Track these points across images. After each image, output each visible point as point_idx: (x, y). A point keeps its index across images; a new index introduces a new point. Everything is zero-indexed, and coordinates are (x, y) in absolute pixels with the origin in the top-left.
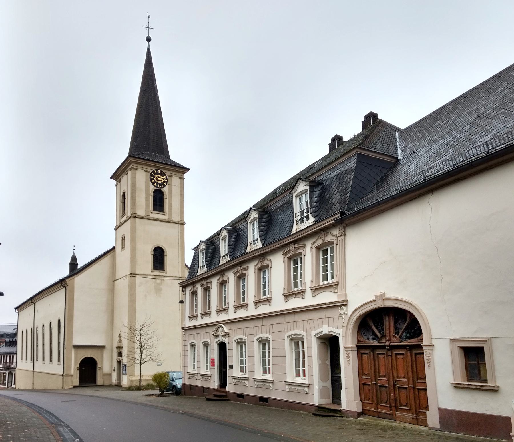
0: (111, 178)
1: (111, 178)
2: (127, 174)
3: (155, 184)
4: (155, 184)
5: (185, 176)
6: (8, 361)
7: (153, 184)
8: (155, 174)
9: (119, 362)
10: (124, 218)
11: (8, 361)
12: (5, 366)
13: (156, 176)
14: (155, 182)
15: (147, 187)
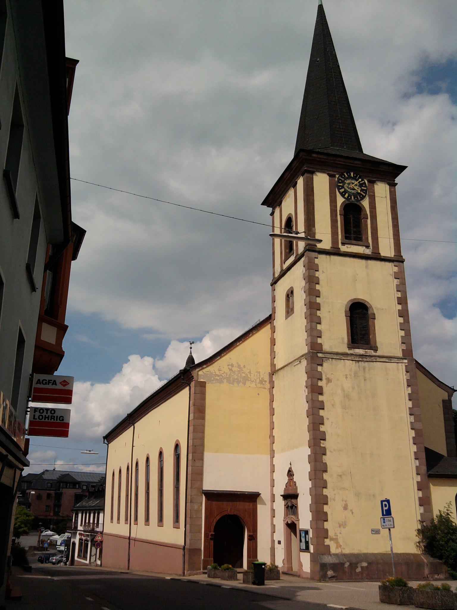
0: (263, 204)
1: (263, 204)
2: (295, 186)
3: (346, 195)
4: (346, 195)
5: (397, 180)
6: (91, 521)
7: (343, 195)
8: (346, 179)
9: (292, 527)
10: (292, 259)
11: (91, 521)
12: (87, 528)
13: (348, 181)
14: (345, 192)
15: (333, 201)
